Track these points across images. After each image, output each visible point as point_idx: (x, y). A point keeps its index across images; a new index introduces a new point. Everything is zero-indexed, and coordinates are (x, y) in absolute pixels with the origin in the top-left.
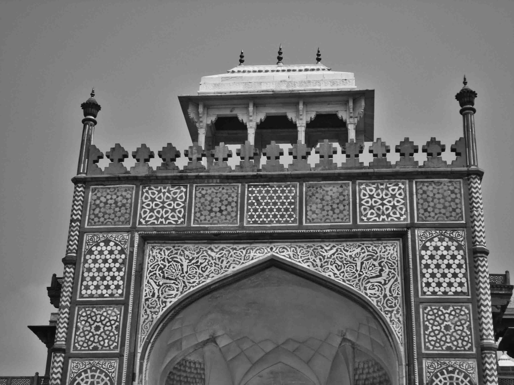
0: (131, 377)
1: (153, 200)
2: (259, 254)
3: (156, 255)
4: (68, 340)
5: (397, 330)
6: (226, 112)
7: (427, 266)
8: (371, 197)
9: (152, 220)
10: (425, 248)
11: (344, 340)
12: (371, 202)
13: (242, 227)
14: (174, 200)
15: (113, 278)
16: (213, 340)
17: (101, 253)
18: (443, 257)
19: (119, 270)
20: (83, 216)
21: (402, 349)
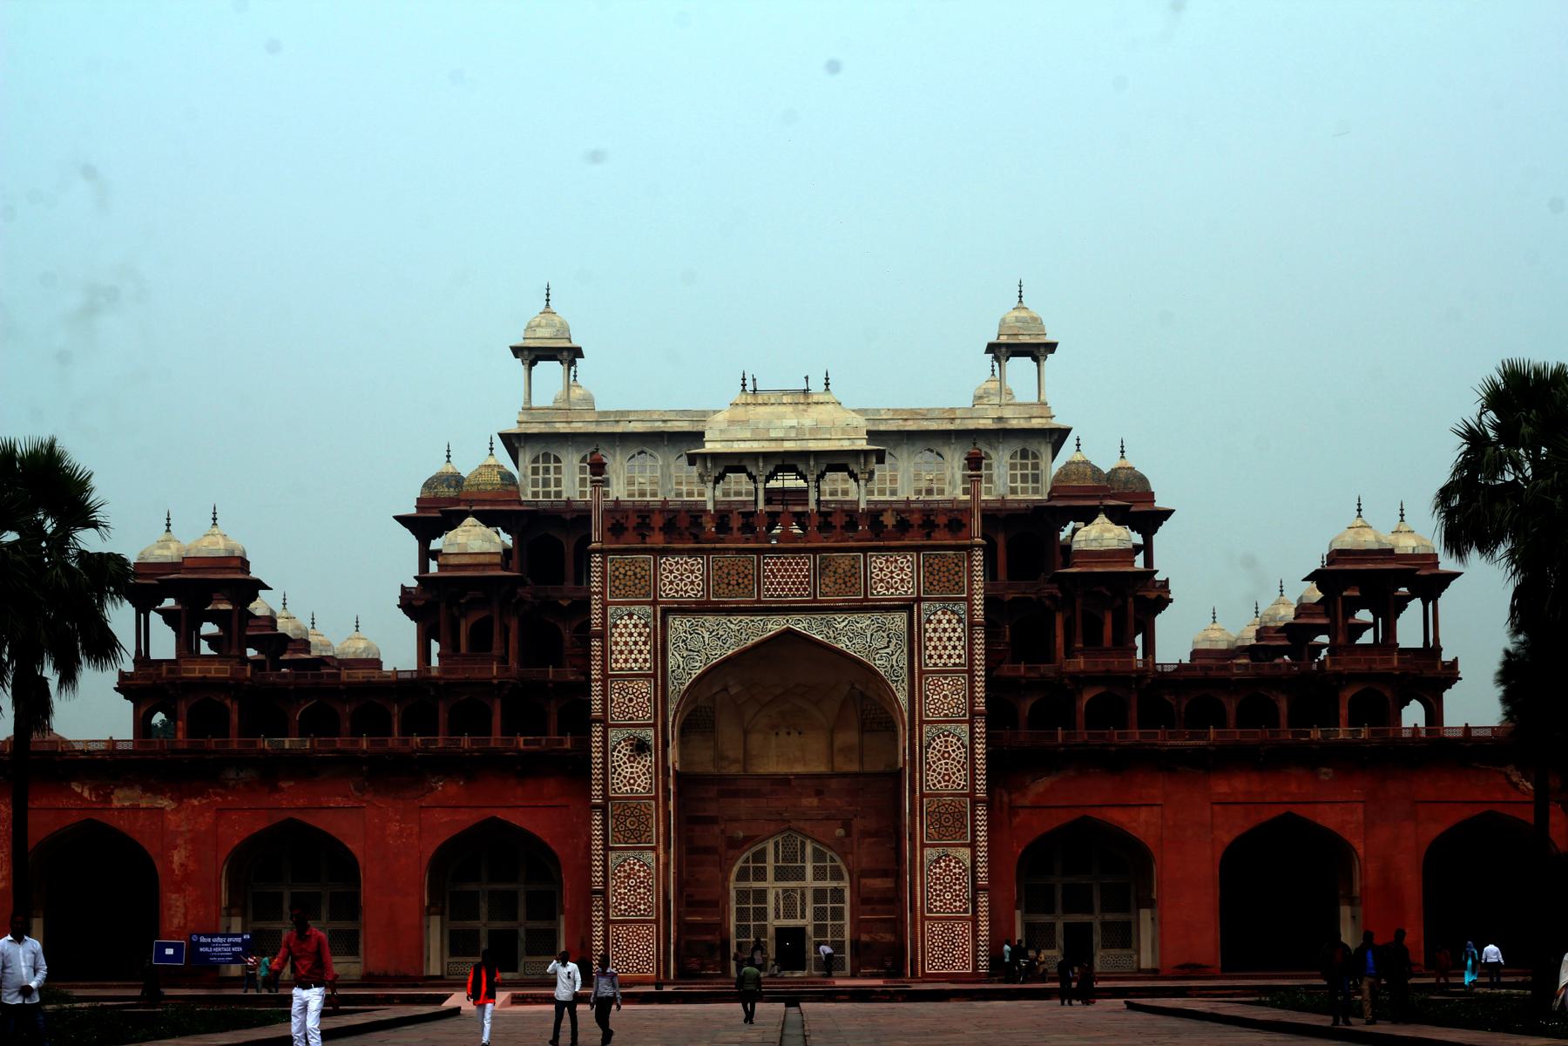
0: (666, 744)
1: (671, 572)
2: (775, 625)
3: (678, 625)
4: (605, 710)
5: (902, 697)
6: (736, 463)
7: (930, 639)
8: (881, 570)
9: (672, 593)
10: (929, 621)
11: (853, 687)
12: (881, 575)
13: (759, 601)
14: (692, 572)
15: (640, 652)
16: (725, 689)
17: (626, 626)
18: (945, 630)
19: (645, 643)
20: (604, 588)
21: (906, 715)
